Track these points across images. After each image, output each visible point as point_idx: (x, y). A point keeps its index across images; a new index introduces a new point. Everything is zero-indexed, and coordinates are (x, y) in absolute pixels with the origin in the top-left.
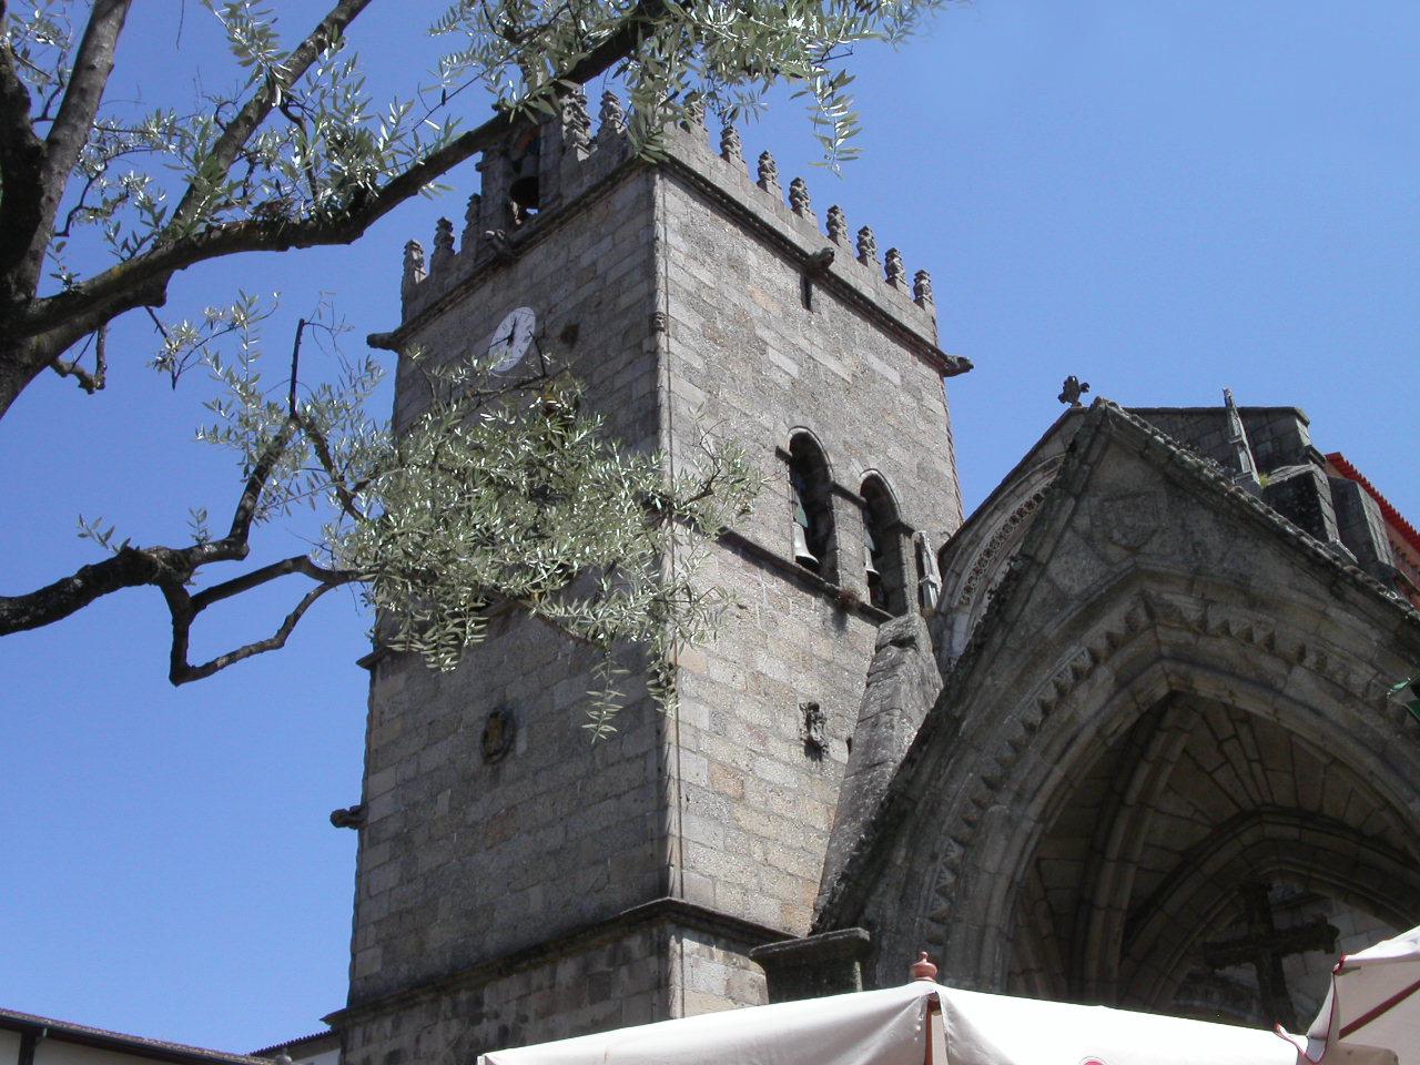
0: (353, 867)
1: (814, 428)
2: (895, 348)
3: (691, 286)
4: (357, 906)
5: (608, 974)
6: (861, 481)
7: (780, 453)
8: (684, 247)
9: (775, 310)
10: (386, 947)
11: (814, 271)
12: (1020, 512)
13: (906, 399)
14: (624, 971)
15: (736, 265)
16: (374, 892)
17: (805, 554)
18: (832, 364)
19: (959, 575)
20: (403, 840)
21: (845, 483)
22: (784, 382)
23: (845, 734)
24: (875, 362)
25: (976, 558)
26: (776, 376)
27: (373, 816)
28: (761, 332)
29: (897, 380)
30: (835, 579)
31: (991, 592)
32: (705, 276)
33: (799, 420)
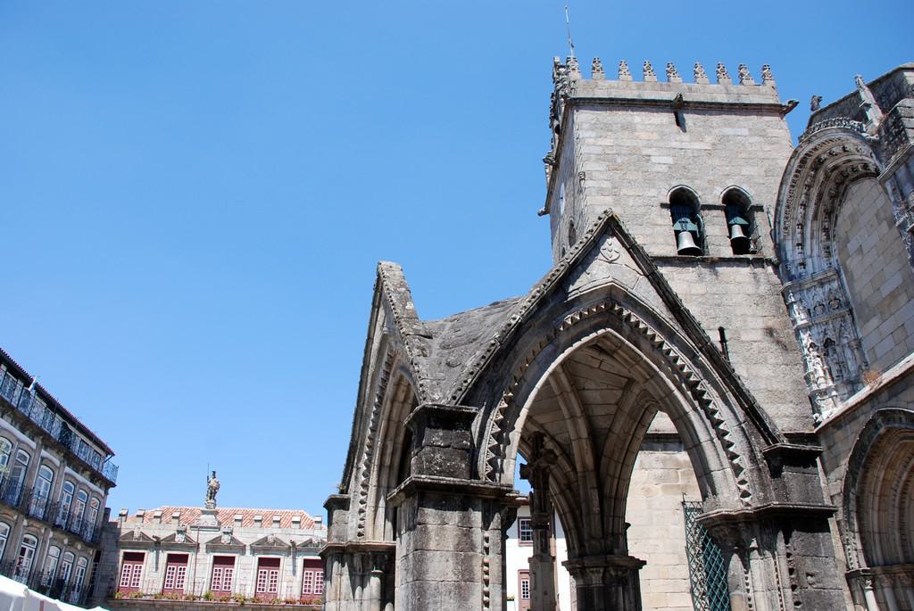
1: (685, 183)
2: (733, 118)
3: (598, 150)
6: (722, 195)
7: (663, 206)
8: (593, 134)
9: (655, 136)
11: (678, 108)
12: (794, 181)
13: (756, 139)
15: (629, 128)
18: (697, 146)
19: (779, 223)
21: (710, 202)
22: (664, 169)
23: (717, 326)
24: (728, 131)
25: (783, 211)
26: (658, 168)
28: (648, 152)
29: (745, 132)
31: (798, 225)
32: (608, 142)
33: (675, 183)
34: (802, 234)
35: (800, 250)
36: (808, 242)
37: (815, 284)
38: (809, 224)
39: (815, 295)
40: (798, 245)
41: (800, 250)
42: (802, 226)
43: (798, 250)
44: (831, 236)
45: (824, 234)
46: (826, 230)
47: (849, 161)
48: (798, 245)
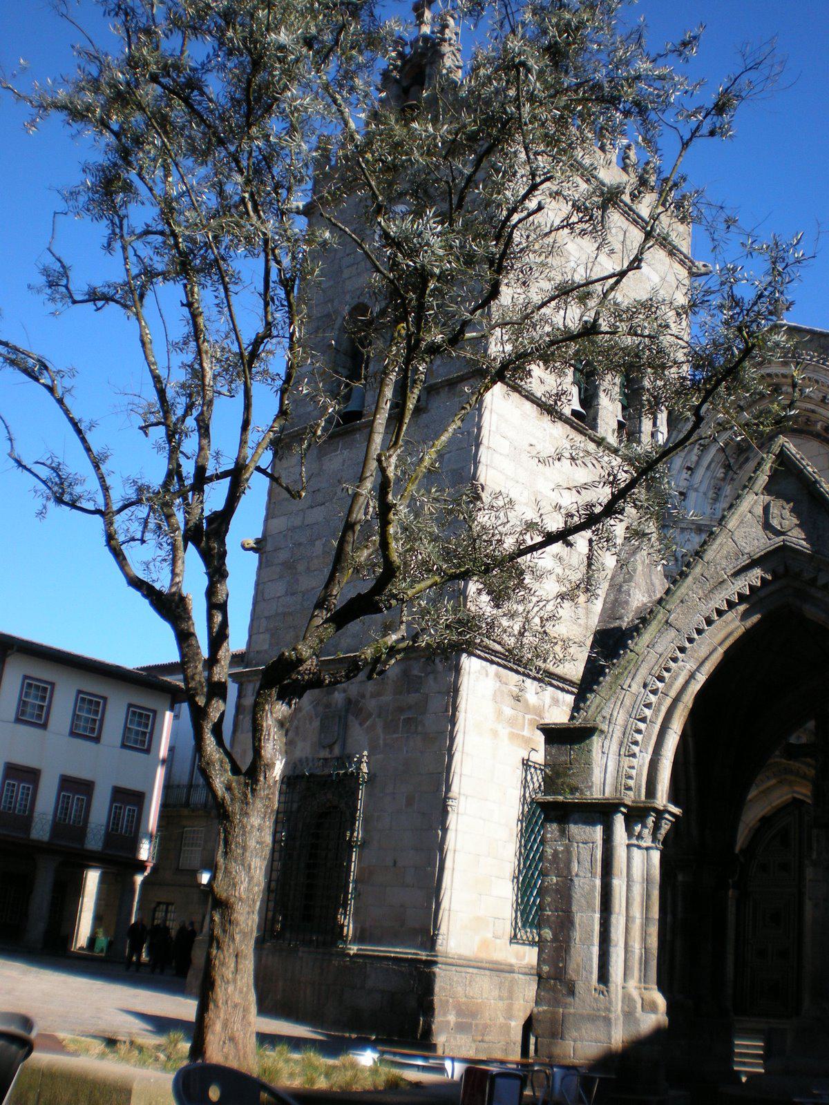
0: (254, 578)
4: (255, 604)
5: (420, 677)
10: (272, 635)
14: (431, 676)
16: (267, 596)
17: (578, 408)
20: (289, 566)
27: (269, 547)
30: (594, 427)
31: (700, 445)
34: (700, 457)
35: (687, 476)
36: (701, 472)
37: (693, 527)
38: (713, 450)
39: (689, 540)
40: (689, 468)
41: (687, 476)
42: (704, 448)
43: (685, 474)
44: (729, 477)
45: (723, 470)
46: (728, 467)
47: (813, 411)
48: (689, 468)
